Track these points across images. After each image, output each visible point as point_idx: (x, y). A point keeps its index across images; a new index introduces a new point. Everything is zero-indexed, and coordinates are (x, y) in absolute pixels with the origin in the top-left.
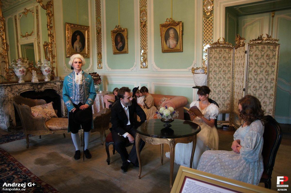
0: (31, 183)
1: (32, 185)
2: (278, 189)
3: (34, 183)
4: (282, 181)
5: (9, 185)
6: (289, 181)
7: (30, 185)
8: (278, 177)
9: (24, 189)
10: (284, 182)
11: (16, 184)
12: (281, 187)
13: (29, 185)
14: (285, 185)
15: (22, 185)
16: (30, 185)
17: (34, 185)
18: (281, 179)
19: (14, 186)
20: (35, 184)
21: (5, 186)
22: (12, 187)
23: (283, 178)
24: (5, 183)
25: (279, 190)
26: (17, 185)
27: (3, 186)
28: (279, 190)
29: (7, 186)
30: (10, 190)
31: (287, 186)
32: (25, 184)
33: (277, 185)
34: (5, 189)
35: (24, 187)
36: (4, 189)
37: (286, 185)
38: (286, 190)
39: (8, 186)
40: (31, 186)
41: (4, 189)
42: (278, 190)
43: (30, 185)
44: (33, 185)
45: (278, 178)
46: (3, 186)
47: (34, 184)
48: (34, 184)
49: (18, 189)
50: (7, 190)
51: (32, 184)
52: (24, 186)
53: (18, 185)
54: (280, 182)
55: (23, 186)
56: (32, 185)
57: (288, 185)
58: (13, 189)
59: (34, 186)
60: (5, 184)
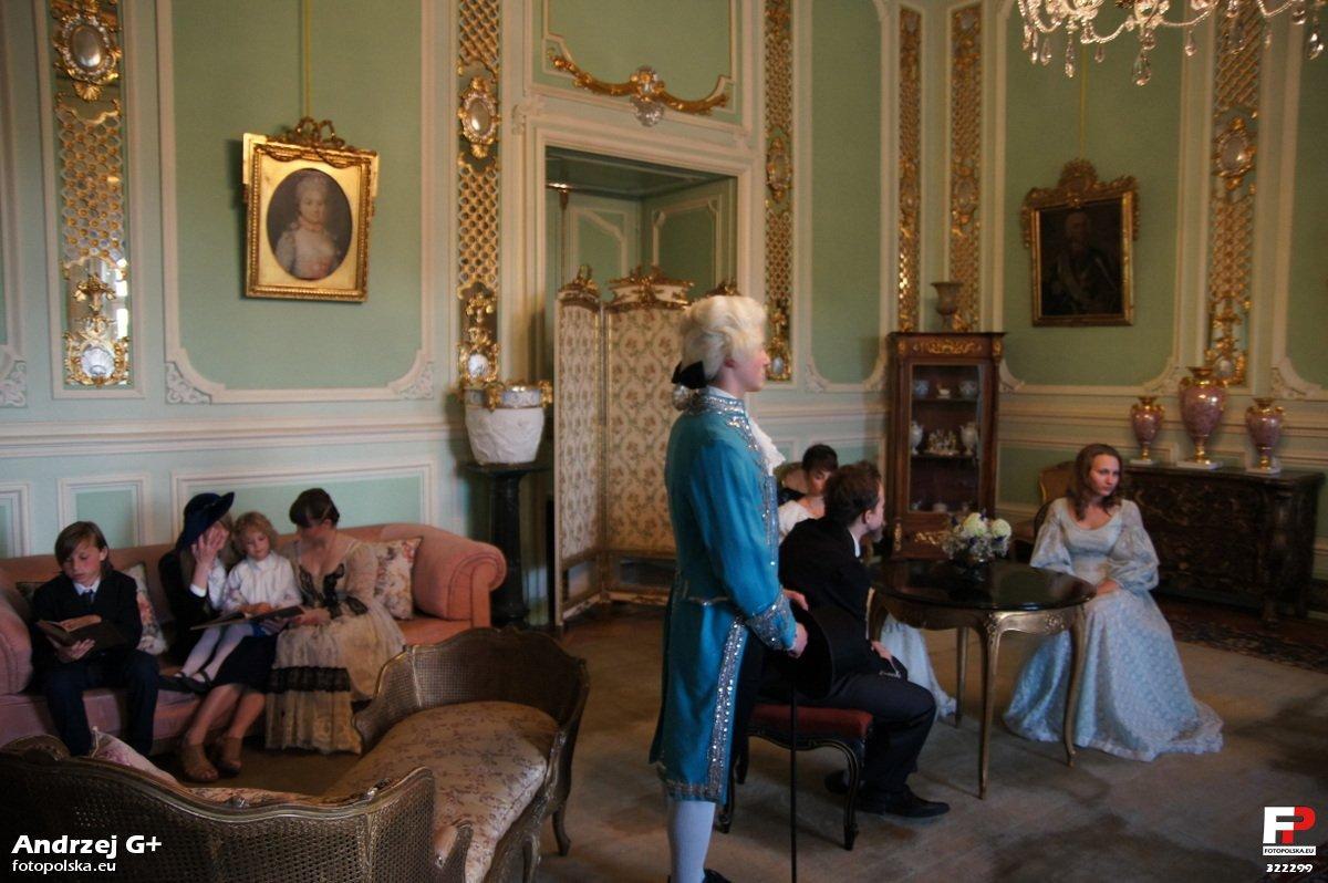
0: (141, 838)
1: (148, 849)
2: (1270, 866)
3: (154, 838)
4: (1289, 826)
5: (42, 847)
6: (1318, 828)
7: (137, 848)
8: (1266, 809)
9: (111, 867)
10: (1295, 832)
12: (1284, 854)
13: (134, 846)
14: (1300, 848)
15: (98, 848)
16: (138, 845)
17: (157, 847)
18: (1280, 819)
19: (64, 850)
20: (159, 844)
21: (23, 850)
22: (53, 858)
23: (1292, 814)
25: (1274, 868)
26: (79, 847)
27: (15, 851)
28: (1274, 868)
29: (30, 851)
30: (44, 868)
31: (1311, 851)
32: (114, 843)
33: (1265, 848)
34: (23, 867)
35: (109, 857)
36: (19, 863)
37: (1304, 848)
38: (1308, 867)
39: (37, 851)
40: (141, 846)
41: (17, 866)
42: (1270, 870)
43: (136, 844)
44: (150, 847)
45: (1271, 813)
46: (15, 851)
47: (154, 844)
48: (154, 844)
49: (82, 867)
50: (33, 867)
51: (148, 844)
52: (109, 853)
53: (81, 846)
54: (1280, 834)
55: (106, 851)
56: (148, 849)
57: (1314, 848)
58: (59, 867)
59: (153, 849)
60: (23, 842)
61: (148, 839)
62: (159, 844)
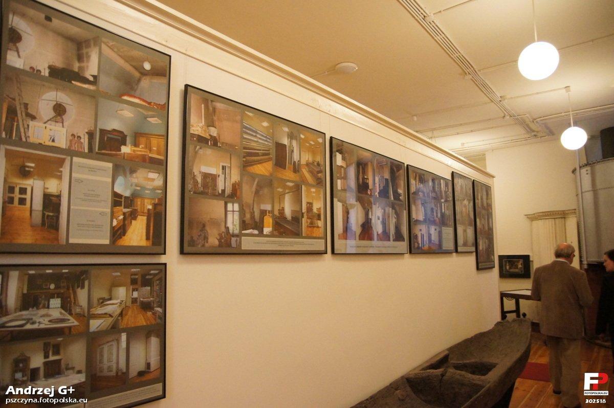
1: (68, 392)
5: (19, 391)
7: (63, 392)
11: (34, 390)
13: (62, 391)
15: (45, 392)
16: (64, 390)
17: (73, 391)
19: (29, 393)
20: (74, 390)
21: (11, 393)
22: (24, 396)
24: (11, 387)
26: (36, 391)
27: (7, 393)
29: (14, 393)
32: (53, 390)
35: (50, 396)
39: (17, 393)
40: (65, 393)
44: (70, 391)
46: (7, 393)
47: (71, 390)
48: (71, 390)
51: (68, 390)
55: (49, 393)
56: (68, 392)
59: (71, 393)
60: (11, 389)
61: (68, 388)
62: (74, 390)
